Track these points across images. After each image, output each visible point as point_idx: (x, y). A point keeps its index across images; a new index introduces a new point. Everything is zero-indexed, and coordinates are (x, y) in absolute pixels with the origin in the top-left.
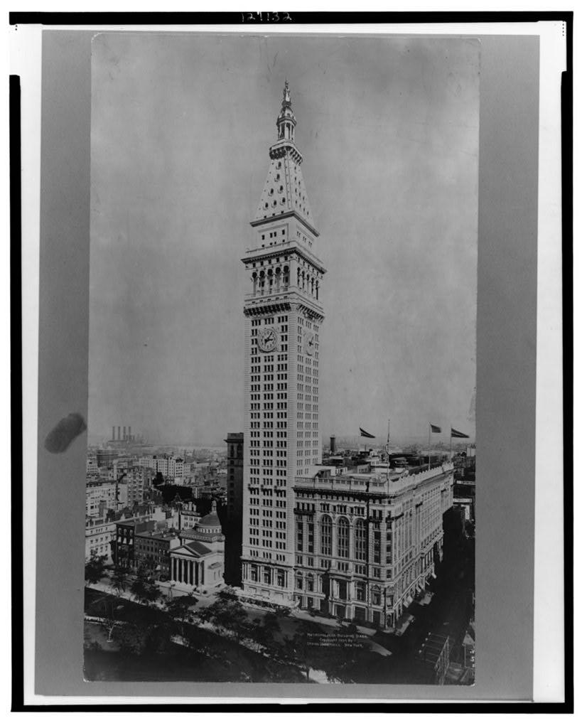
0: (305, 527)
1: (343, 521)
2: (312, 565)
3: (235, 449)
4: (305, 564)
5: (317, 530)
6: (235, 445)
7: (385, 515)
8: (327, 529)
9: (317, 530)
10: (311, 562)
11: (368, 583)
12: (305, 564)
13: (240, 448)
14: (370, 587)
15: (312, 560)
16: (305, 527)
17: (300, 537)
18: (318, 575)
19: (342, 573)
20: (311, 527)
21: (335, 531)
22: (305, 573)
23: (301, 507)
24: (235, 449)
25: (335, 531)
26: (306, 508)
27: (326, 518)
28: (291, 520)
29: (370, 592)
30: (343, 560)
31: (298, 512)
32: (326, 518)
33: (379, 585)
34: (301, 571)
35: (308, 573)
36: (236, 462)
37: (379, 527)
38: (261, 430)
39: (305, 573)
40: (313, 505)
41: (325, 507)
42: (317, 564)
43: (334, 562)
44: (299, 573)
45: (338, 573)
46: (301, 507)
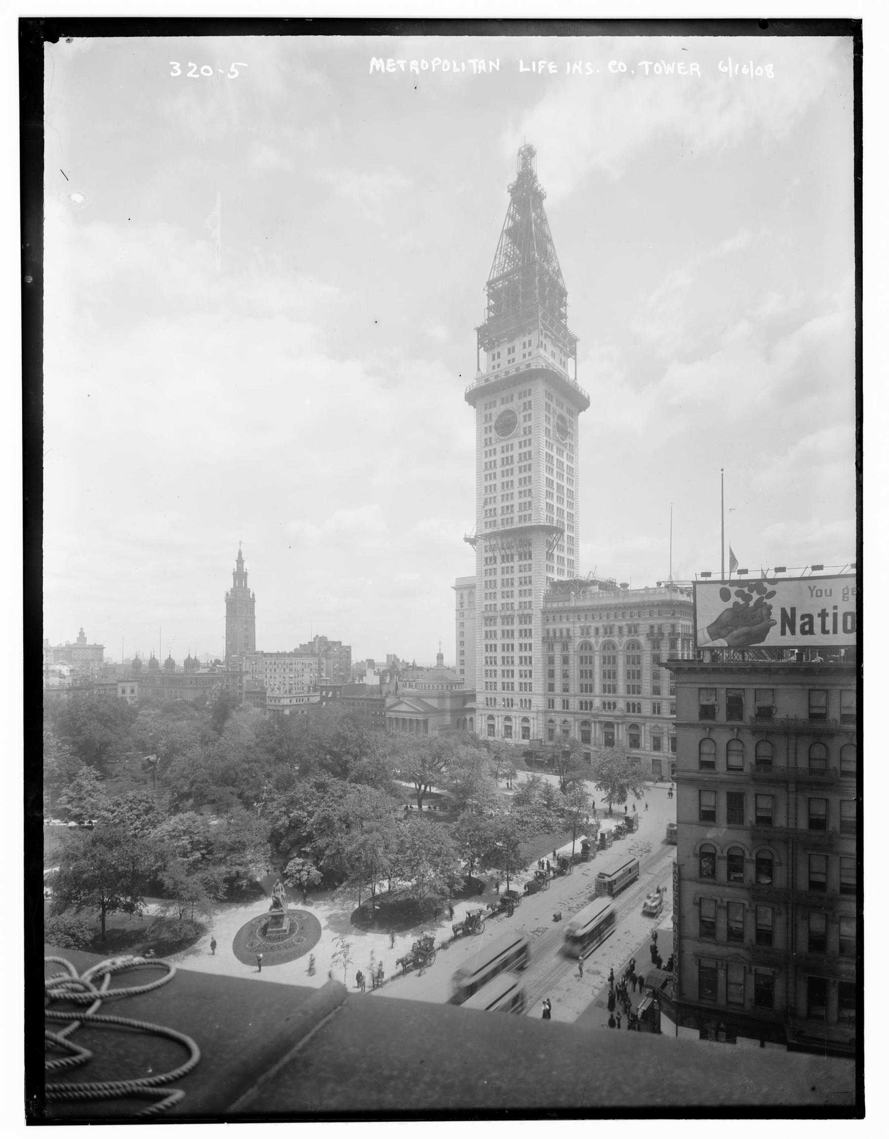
0: (558, 660)
1: (609, 646)
2: (568, 708)
3: (465, 597)
4: (558, 706)
5: (574, 661)
6: (466, 593)
7: (667, 630)
8: (587, 660)
9: (574, 661)
10: (566, 704)
11: (644, 724)
12: (558, 706)
13: (471, 594)
14: (648, 728)
15: (568, 701)
16: (558, 660)
17: (551, 674)
18: (575, 720)
19: (609, 713)
20: (565, 660)
21: (597, 661)
22: (558, 720)
23: (551, 634)
24: (465, 597)
25: (597, 661)
26: (558, 634)
27: (586, 646)
28: (537, 653)
29: (647, 733)
30: (610, 698)
31: (549, 641)
32: (586, 646)
33: (660, 725)
34: (553, 718)
35: (563, 719)
36: (466, 613)
37: (658, 647)
38: (499, 589)
39: (558, 720)
40: (568, 630)
41: (585, 631)
42: (574, 705)
43: (597, 703)
44: (551, 721)
45: (604, 713)
46: (551, 634)
